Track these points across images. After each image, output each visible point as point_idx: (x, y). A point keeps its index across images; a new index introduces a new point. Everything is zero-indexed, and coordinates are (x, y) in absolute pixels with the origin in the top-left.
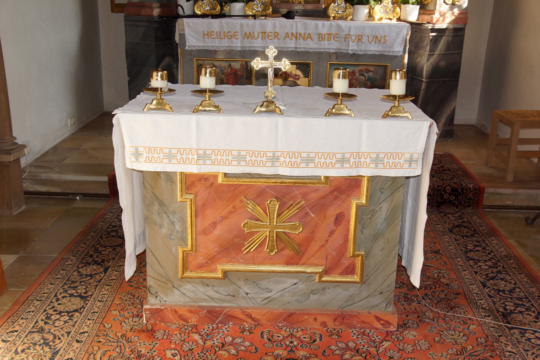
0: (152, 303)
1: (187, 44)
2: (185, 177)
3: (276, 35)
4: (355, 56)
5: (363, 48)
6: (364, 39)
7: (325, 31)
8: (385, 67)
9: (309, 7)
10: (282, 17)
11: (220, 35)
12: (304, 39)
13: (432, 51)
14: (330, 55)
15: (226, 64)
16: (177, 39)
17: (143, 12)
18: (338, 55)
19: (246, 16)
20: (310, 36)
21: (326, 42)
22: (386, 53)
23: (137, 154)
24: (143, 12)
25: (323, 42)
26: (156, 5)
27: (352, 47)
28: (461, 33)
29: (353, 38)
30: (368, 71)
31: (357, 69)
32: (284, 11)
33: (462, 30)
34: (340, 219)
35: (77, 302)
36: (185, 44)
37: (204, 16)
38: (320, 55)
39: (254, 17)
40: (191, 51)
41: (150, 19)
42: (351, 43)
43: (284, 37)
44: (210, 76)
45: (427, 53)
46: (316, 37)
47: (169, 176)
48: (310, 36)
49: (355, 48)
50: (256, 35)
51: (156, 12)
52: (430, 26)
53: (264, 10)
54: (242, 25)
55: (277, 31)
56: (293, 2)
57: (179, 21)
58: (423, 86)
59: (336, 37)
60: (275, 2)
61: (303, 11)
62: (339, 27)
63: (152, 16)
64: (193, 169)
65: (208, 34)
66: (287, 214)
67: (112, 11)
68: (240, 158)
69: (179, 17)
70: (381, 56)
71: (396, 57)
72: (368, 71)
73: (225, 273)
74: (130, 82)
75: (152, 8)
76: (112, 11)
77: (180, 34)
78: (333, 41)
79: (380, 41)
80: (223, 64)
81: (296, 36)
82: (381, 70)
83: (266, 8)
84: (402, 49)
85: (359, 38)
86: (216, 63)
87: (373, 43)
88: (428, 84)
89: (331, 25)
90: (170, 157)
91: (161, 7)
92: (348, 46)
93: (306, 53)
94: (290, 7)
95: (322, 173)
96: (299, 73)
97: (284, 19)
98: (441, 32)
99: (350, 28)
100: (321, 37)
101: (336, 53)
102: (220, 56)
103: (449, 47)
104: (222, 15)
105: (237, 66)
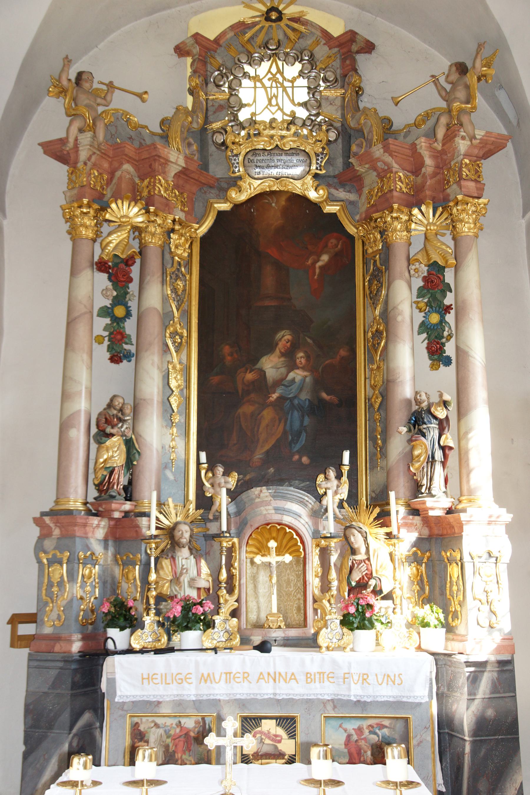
1: (118, 693)
3: (246, 676)
4: (360, 704)
6: (371, 679)
7: (314, 669)
8: (406, 720)
9: (293, 633)
10: (254, 649)
11: (165, 679)
12: (285, 681)
13: (472, 693)
14: (324, 703)
15: (174, 721)
18: (335, 703)
21: (317, 684)
22: (405, 700)
24: (57, 648)
25: (312, 685)
26: (77, 636)
28: (509, 667)
29: (356, 677)
30: (382, 727)
31: (365, 724)
32: (257, 640)
33: (510, 662)
37: (142, 651)
39: (215, 650)
40: (124, 703)
41: (67, 659)
42: (352, 684)
43: (256, 678)
44: (151, 760)
45: (466, 696)
46: (303, 678)
49: (360, 692)
50: (217, 678)
51: (76, 647)
52: (462, 659)
53: (229, 640)
54: (197, 663)
55: (247, 670)
56: (269, 626)
57: (109, 660)
58: (468, 748)
59: (331, 676)
60: (245, 627)
61: (284, 640)
62: (334, 662)
63: (70, 652)
65: (149, 678)
67: (12, 645)
69: (108, 653)
70: (399, 704)
71: (420, 704)
72: (382, 727)
74: (26, 756)
75: (70, 642)
76: (12, 645)
77: (108, 679)
78: (327, 683)
79: (394, 682)
80: (171, 722)
81: (275, 677)
82: (400, 725)
83: (231, 637)
84: (426, 693)
85: (364, 678)
86: (159, 721)
87: (384, 684)
88: (474, 743)
89: (323, 660)
91: (84, 638)
92: (349, 689)
93: (290, 702)
94: (266, 634)
96: (280, 731)
97: (257, 652)
98: (481, 666)
99: (350, 664)
100: (309, 677)
101: (332, 700)
102: (165, 710)
103: (495, 688)
104: (171, 650)
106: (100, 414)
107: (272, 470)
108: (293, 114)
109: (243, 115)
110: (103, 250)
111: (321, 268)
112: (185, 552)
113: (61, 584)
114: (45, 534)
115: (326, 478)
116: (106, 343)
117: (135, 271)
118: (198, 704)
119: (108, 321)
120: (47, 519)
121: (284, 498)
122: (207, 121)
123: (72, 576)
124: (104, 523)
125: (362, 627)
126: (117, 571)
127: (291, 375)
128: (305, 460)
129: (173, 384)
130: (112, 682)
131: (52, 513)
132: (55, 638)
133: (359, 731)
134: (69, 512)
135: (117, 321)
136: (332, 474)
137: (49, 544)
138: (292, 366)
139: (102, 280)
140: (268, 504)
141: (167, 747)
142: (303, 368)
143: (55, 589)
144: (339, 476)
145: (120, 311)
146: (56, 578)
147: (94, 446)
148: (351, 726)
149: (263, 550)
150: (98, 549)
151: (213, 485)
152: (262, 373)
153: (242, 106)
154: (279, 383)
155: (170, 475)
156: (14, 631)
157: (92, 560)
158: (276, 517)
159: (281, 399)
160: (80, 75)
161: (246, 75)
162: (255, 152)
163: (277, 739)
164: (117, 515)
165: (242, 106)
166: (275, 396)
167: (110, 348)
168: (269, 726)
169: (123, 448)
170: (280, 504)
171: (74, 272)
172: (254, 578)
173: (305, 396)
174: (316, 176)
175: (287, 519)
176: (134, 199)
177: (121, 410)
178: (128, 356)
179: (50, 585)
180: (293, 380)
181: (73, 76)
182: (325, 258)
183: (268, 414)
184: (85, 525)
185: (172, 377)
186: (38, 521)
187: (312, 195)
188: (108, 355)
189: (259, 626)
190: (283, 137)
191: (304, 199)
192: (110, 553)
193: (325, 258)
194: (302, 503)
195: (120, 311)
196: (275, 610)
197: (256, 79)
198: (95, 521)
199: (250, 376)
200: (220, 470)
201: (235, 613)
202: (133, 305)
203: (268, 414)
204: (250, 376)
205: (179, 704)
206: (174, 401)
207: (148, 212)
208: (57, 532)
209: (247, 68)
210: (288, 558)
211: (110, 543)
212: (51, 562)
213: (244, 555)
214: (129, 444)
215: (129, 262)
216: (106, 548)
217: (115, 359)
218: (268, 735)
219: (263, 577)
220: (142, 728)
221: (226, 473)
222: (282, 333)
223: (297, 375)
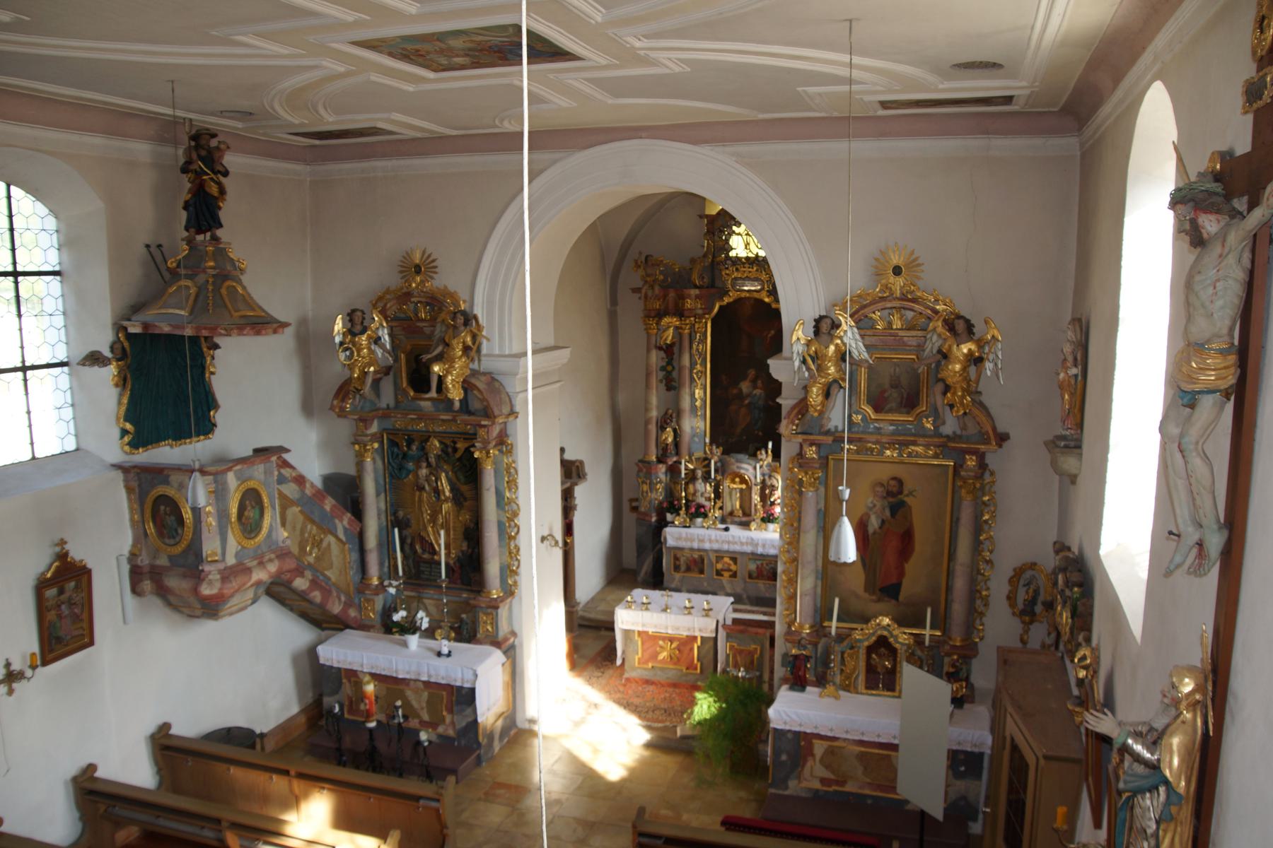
0: (626, 675)
2: (639, 632)
3: (717, 541)
4: (762, 555)
5: (766, 551)
6: (767, 546)
11: (686, 539)
16: (662, 539)
17: (647, 518)
18: (753, 554)
19: (703, 527)
20: (736, 543)
23: (622, 622)
26: (654, 514)
27: (760, 550)
31: (764, 562)
34: (692, 649)
35: (600, 674)
36: (666, 543)
38: (743, 554)
47: (634, 631)
48: (736, 543)
51: (654, 519)
64: (640, 629)
65: (679, 539)
66: (673, 646)
68: (656, 626)
73: (653, 667)
75: (651, 517)
80: (688, 555)
81: (729, 542)
85: (764, 546)
90: (633, 624)
93: (734, 552)
95: (685, 633)
96: (731, 562)
102: (686, 551)
105: (696, 556)
106: (662, 418)
107: (745, 437)
108: (757, 254)
109: (732, 254)
110: (661, 338)
111: (771, 337)
112: (700, 481)
113: (647, 492)
114: (640, 470)
115: (761, 454)
116: (664, 381)
117: (676, 349)
118: (699, 550)
119: (664, 373)
120: (640, 464)
121: (741, 462)
122: (714, 257)
123: (651, 491)
124: (664, 466)
125: (769, 522)
126: (673, 486)
127: (755, 392)
128: (760, 433)
129: (697, 396)
130: (665, 539)
131: (641, 461)
132: (647, 514)
133: (762, 564)
134: (649, 463)
135: (669, 373)
136: (763, 452)
137: (641, 474)
138: (755, 387)
139: (662, 354)
140: (733, 464)
141: (687, 564)
142: (761, 389)
143: (645, 494)
144: (767, 453)
145: (669, 368)
146: (645, 489)
147: (660, 432)
148: (759, 563)
149: (733, 481)
150: (662, 476)
151: (711, 453)
152: (741, 390)
153: (732, 249)
154: (749, 395)
155: (696, 439)
156: (631, 504)
157: (661, 482)
158: (738, 470)
159: (750, 403)
160: (647, 257)
161: (734, 232)
162: (736, 279)
163: (729, 565)
164: (670, 463)
165: (732, 249)
166: (747, 402)
167: (666, 385)
168: (727, 560)
169: (672, 433)
170: (739, 464)
171: (648, 351)
172: (730, 494)
173: (761, 403)
174: (768, 291)
175: (742, 471)
176: (674, 315)
177: (671, 416)
178: (674, 388)
179: (643, 492)
180: (755, 395)
181: (643, 259)
182: (773, 332)
183: (743, 410)
184: (656, 469)
185: (697, 391)
186: (637, 465)
187: (767, 300)
188: (665, 388)
189: (731, 514)
190: (750, 272)
191: (762, 301)
192: (668, 478)
193: (773, 332)
194: (749, 464)
195: (669, 368)
196: (738, 506)
197: (739, 234)
198: (661, 466)
199: (735, 391)
200: (714, 447)
201: (721, 508)
202: (675, 364)
203: (743, 410)
204: (735, 391)
205: (692, 549)
206: (698, 403)
207: (681, 320)
208: (644, 470)
209: (734, 228)
210: (744, 486)
211: (668, 474)
212: (643, 482)
213: (725, 485)
214: (675, 431)
215: (673, 344)
216: (666, 476)
217: (669, 388)
218: (726, 563)
219: (734, 492)
220: (678, 556)
221: (717, 447)
222: (749, 372)
223: (758, 392)
